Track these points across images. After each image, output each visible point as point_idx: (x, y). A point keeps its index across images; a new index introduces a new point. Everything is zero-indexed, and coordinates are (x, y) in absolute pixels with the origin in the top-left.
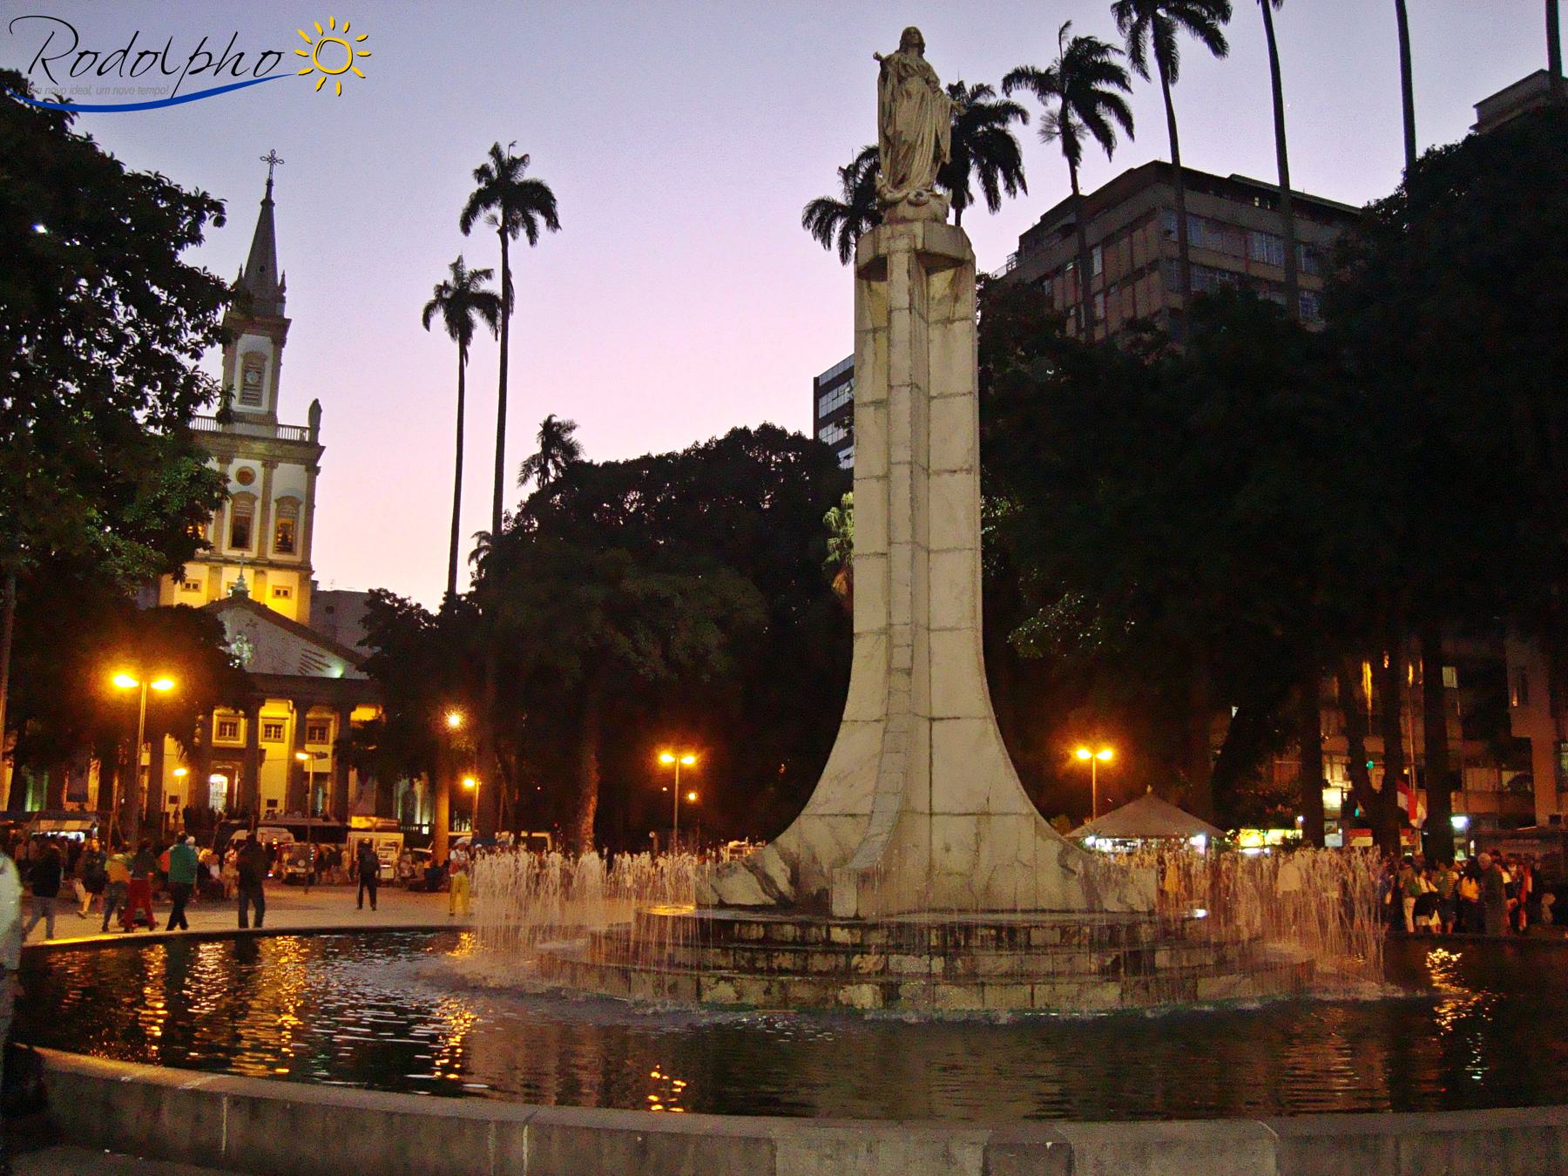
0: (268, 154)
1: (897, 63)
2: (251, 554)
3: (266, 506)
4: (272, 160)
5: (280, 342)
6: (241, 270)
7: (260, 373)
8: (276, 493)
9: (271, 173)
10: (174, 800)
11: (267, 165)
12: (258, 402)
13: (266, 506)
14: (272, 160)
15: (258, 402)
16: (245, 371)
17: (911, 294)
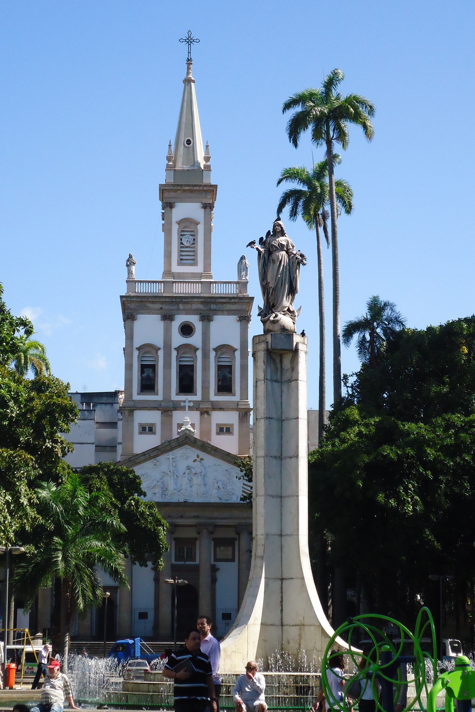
0: (185, 36)
1: (269, 244)
2: (198, 397)
3: (206, 356)
4: (189, 41)
5: (208, 207)
6: (170, 146)
7: (194, 235)
8: (214, 344)
9: (189, 53)
10: (143, 616)
11: (185, 46)
12: (194, 262)
13: (206, 356)
14: (189, 41)
15: (194, 262)
16: (181, 235)
17: (265, 372)
